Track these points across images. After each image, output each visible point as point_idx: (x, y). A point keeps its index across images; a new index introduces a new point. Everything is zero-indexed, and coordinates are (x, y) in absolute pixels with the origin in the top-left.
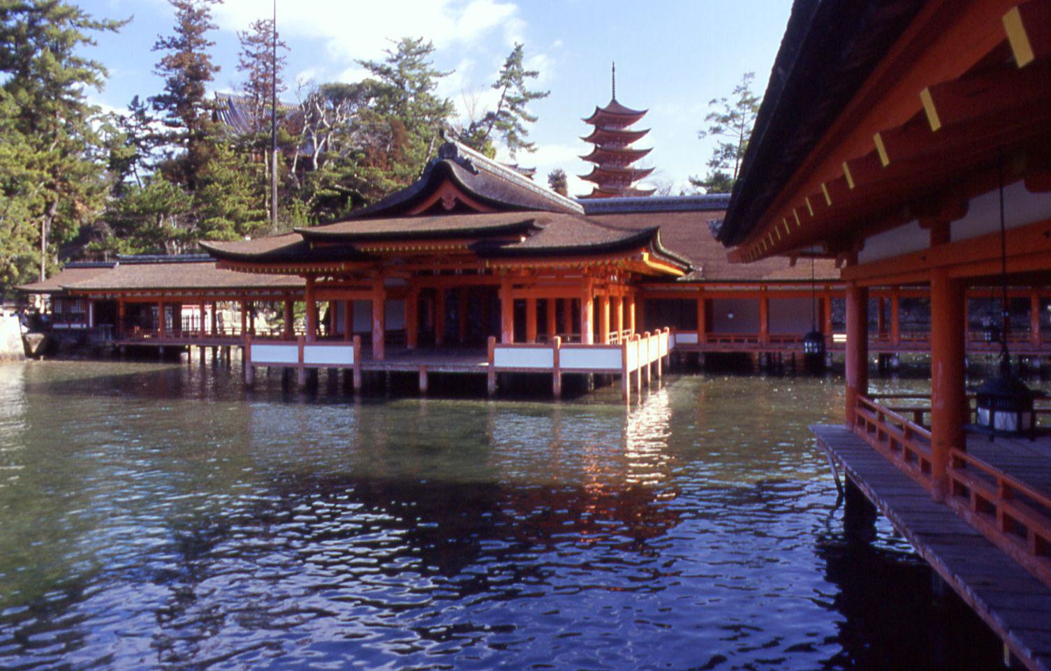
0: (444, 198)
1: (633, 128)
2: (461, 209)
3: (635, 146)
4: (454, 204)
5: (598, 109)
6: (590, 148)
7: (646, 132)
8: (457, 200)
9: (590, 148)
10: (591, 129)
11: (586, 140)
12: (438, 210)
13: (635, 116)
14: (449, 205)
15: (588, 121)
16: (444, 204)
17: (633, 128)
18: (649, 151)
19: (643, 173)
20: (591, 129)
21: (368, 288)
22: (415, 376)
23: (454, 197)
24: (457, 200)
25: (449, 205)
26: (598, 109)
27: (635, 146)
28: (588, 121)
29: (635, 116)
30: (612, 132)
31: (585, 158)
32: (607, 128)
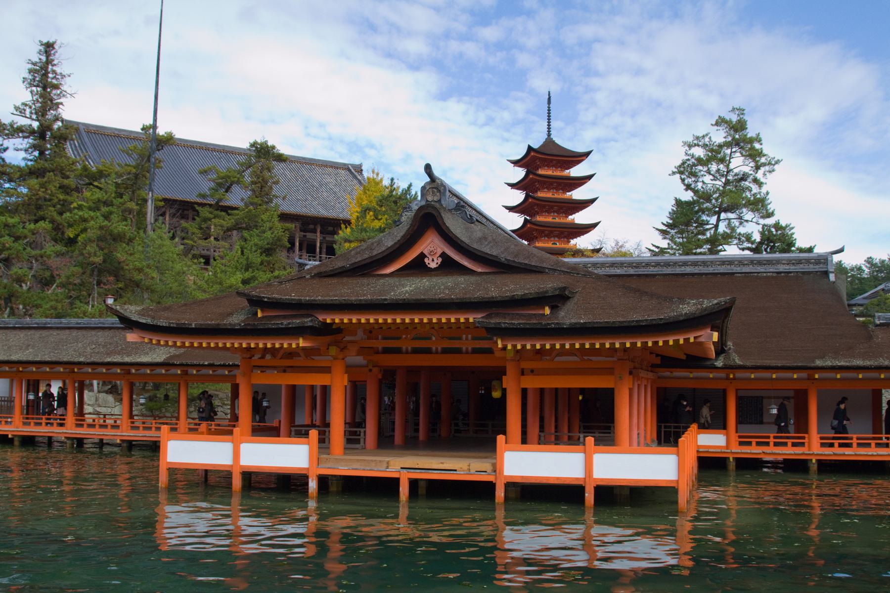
0: (426, 252)
1: (576, 172)
2: (448, 266)
3: (578, 194)
4: (440, 260)
5: (530, 149)
6: (518, 197)
8: (443, 255)
9: (518, 197)
10: (519, 174)
11: (513, 186)
12: (418, 266)
13: (577, 158)
14: (433, 263)
15: (516, 163)
16: (426, 260)
17: (576, 172)
18: (592, 201)
20: (519, 174)
21: (327, 370)
23: (439, 252)
24: (443, 255)
25: (433, 263)
26: (530, 149)
27: (578, 194)
28: (516, 163)
29: (577, 158)
30: (548, 175)
31: (511, 209)
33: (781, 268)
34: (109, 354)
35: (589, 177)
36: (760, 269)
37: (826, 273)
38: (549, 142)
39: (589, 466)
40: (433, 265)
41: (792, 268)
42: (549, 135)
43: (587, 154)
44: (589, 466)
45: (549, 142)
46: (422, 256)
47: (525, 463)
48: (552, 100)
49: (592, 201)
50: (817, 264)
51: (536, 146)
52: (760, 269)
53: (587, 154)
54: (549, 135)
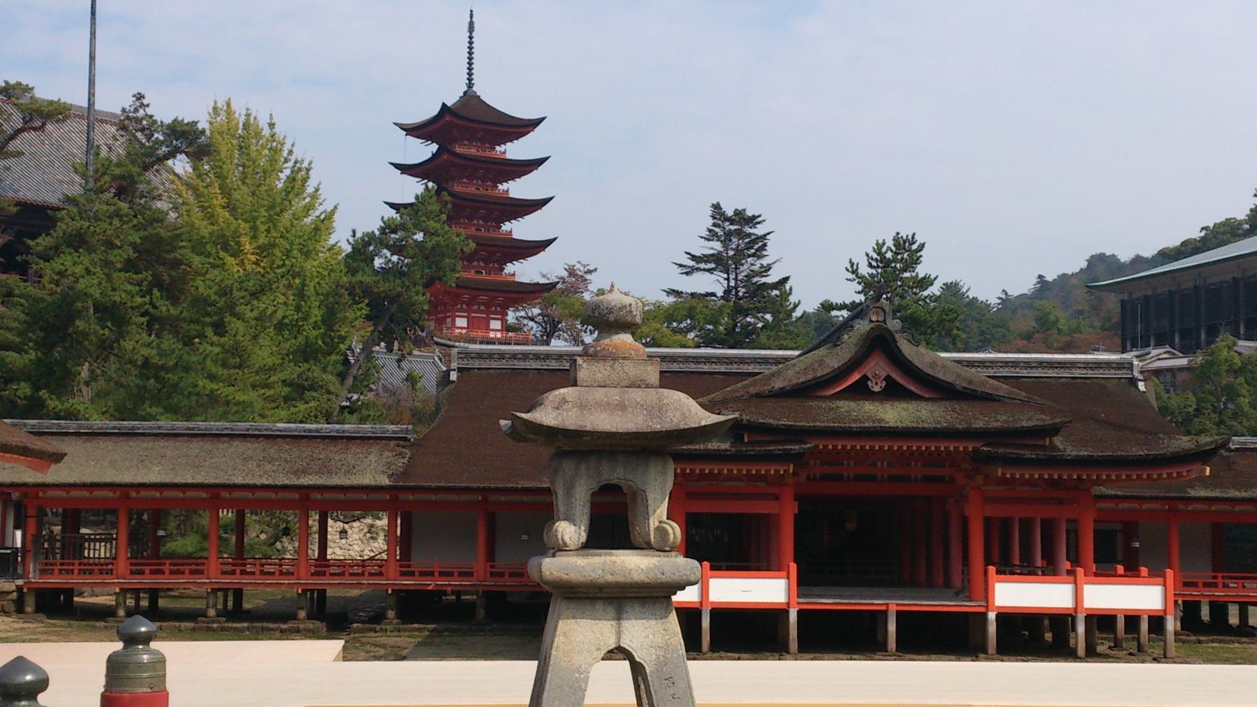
1: (514, 150)
2: (893, 392)
3: (518, 189)
7: (539, 162)
8: (888, 379)
10: (422, 151)
12: (860, 391)
15: (413, 130)
16: (869, 383)
17: (514, 150)
19: (538, 247)
20: (422, 151)
22: (884, 614)
23: (884, 374)
24: (888, 379)
27: (518, 189)
28: (413, 130)
32: (458, 150)
33: (1077, 373)
34: (304, 472)
35: (539, 162)
36: (1051, 373)
37: (1133, 382)
38: (470, 98)
39: (1078, 596)
40: (877, 389)
41: (1090, 373)
42: (470, 85)
43: (535, 123)
44: (1078, 596)
45: (470, 98)
46: (865, 379)
47: (1013, 594)
48: (476, 26)
49: (544, 202)
50: (1119, 369)
51: (449, 104)
52: (1051, 373)
53: (537, 122)
54: (470, 85)
